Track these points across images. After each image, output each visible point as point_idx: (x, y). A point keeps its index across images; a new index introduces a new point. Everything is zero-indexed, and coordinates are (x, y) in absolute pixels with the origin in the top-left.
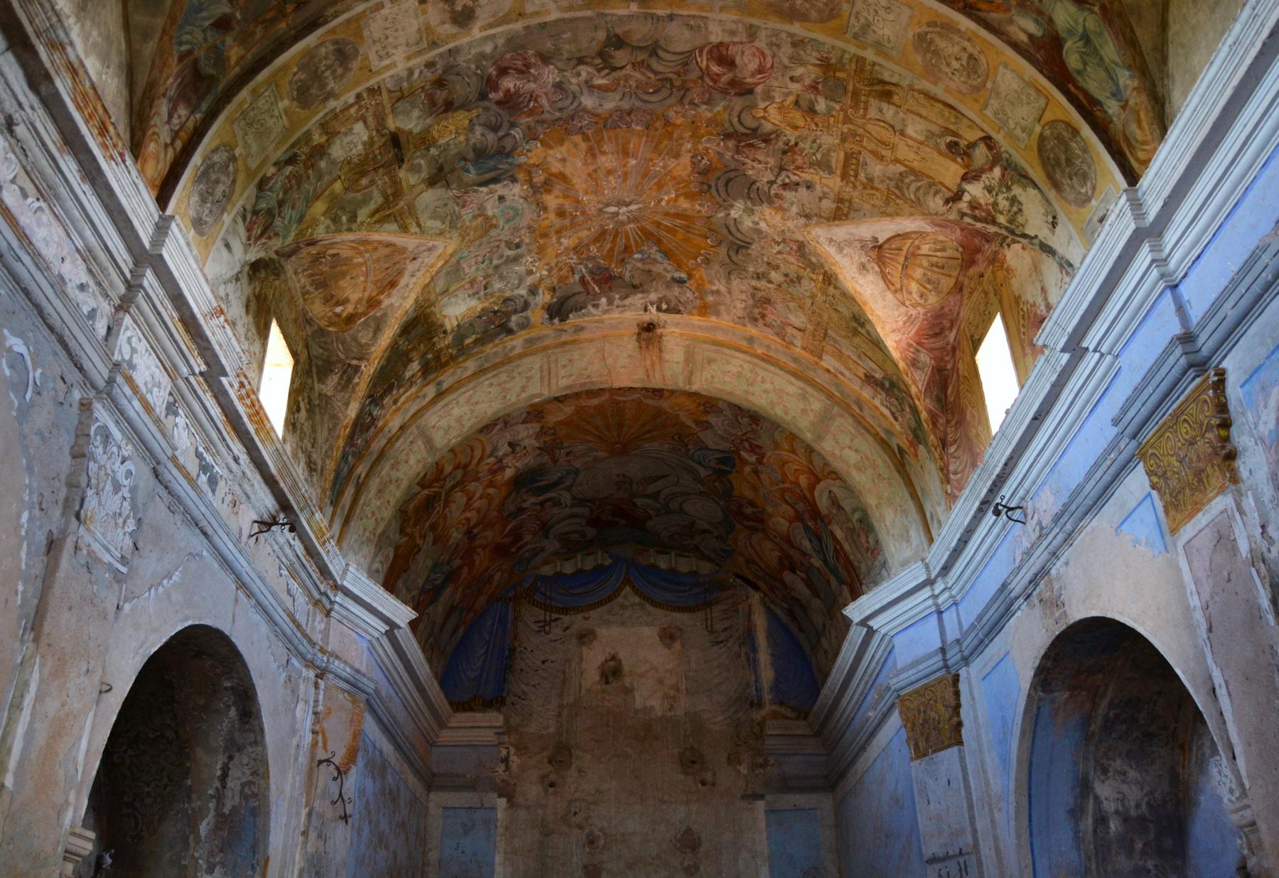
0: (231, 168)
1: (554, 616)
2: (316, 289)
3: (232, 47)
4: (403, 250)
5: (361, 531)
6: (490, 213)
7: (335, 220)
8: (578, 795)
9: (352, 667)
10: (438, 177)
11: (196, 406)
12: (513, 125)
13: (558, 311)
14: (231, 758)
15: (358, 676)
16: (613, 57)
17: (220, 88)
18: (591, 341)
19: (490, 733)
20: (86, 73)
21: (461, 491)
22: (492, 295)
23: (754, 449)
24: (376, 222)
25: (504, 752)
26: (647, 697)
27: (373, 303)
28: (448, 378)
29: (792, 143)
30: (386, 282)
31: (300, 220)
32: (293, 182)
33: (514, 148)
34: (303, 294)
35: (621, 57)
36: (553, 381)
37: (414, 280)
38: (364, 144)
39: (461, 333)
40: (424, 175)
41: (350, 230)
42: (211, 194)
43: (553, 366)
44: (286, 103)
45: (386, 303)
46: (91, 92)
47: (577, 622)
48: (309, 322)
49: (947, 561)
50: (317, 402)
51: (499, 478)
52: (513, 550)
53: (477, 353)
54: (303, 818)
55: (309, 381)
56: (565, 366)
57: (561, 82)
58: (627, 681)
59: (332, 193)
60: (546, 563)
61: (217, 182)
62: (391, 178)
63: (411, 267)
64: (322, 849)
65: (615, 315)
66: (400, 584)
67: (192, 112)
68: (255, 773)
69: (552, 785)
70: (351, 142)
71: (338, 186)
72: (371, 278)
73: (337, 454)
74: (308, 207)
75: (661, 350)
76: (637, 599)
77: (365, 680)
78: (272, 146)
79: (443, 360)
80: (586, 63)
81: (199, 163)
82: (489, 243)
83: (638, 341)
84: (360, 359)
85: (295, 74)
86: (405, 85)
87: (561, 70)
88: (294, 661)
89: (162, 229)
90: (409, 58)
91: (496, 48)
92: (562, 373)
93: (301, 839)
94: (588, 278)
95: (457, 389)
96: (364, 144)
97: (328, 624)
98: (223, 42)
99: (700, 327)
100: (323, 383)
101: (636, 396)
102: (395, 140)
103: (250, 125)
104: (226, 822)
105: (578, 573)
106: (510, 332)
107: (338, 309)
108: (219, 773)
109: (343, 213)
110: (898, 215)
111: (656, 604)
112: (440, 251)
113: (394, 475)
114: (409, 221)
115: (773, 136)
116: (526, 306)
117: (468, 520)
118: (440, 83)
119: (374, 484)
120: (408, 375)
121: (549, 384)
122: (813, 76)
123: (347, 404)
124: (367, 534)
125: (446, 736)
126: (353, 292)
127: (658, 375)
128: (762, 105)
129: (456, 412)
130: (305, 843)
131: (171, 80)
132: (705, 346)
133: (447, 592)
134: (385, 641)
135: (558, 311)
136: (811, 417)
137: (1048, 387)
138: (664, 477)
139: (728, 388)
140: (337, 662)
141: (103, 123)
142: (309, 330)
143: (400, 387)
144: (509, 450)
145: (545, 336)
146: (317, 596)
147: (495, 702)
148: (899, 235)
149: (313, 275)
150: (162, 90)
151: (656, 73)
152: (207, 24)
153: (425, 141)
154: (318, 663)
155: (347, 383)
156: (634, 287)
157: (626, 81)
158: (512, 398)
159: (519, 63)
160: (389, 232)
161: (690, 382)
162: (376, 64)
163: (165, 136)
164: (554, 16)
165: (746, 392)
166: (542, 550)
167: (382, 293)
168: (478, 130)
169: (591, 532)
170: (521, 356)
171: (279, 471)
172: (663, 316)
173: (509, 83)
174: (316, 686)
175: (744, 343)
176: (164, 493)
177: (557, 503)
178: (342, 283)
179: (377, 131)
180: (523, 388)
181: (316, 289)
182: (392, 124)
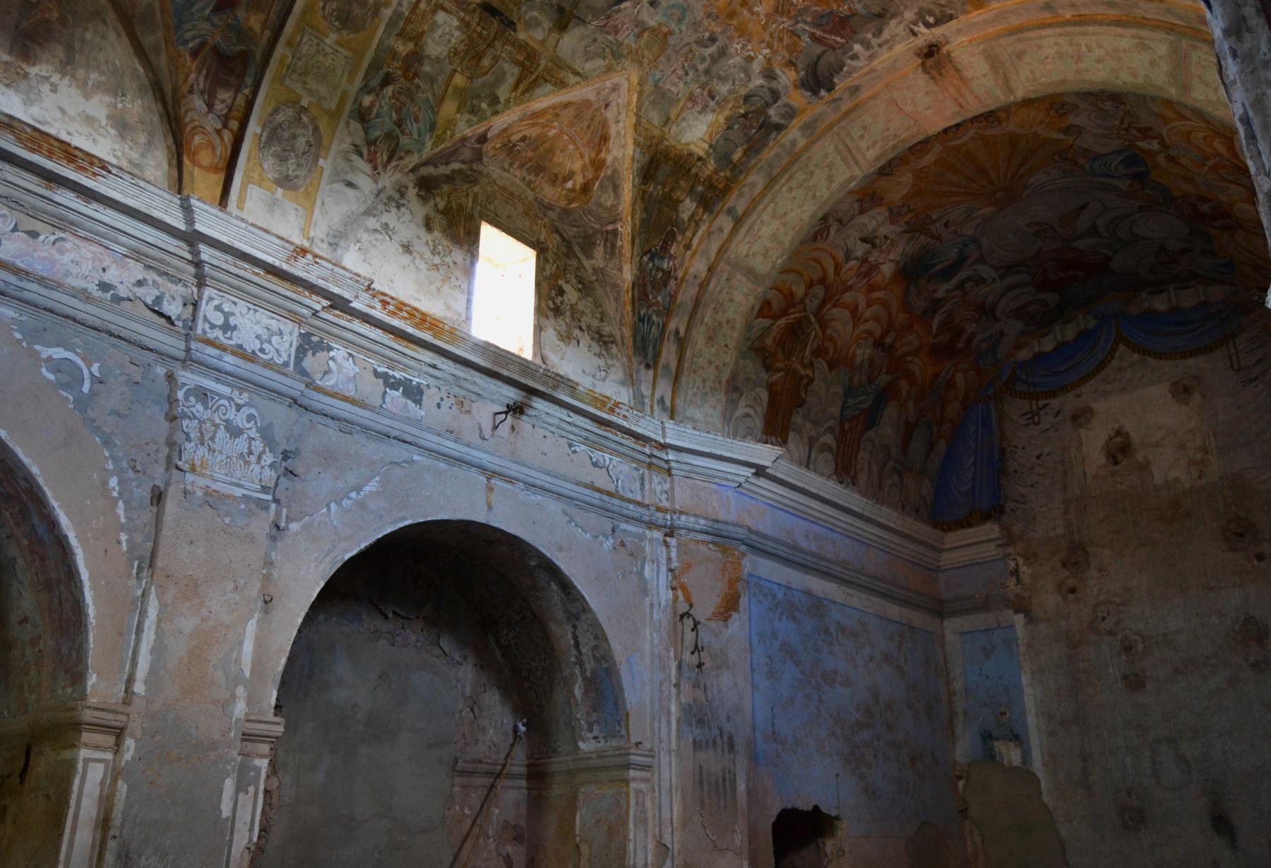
0: (305, 119)
1: (1041, 403)
2: (537, 175)
3: (248, 19)
4: (587, 103)
5: (699, 384)
6: (652, 23)
7: (474, 111)
8: (1101, 598)
9: (706, 519)
13: (817, 80)
14: (575, 627)
15: (720, 526)
17: (258, 58)
18: (873, 97)
19: (992, 546)
20: (20, 121)
21: (835, 306)
22: (725, 99)
23: (1147, 133)
24: (523, 93)
25: (1012, 564)
26: (1168, 468)
27: (598, 165)
28: (738, 201)
30: (597, 141)
31: (433, 127)
32: (402, 98)
36: (859, 158)
37: (621, 125)
38: (458, 28)
39: (721, 153)
40: (547, 24)
41: (496, 113)
42: (293, 150)
43: (848, 141)
44: (332, 38)
45: (609, 159)
46: (36, 134)
47: (1068, 402)
48: (550, 207)
50: (594, 278)
51: (877, 278)
52: (960, 345)
53: (756, 164)
54: (674, 671)
55: (574, 262)
56: (862, 137)
58: (1140, 456)
59: (456, 88)
60: (1019, 347)
61: (294, 137)
62: (513, 44)
63: (610, 114)
64: (702, 698)
65: (885, 56)
66: (797, 419)
67: (237, 91)
68: (596, 637)
69: (1073, 591)
70: (444, 34)
71: (459, 80)
72: (579, 143)
73: (629, 319)
74: (435, 113)
75: (957, 70)
76: (1136, 357)
77: (730, 528)
78: (344, 80)
79: (721, 186)
81: (258, 131)
82: (677, 52)
83: (926, 72)
84: (614, 222)
85: (324, 8)
88: (624, 526)
89: (187, 209)
92: (864, 144)
93: (674, 690)
94: (818, 33)
95: (755, 207)
96: (458, 28)
97: (672, 482)
98: (236, 19)
99: (986, 22)
100: (592, 258)
101: (972, 132)
103: (305, 73)
104: (591, 684)
105: (1060, 347)
106: (779, 128)
107: (569, 184)
108: (572, 642)
109: (479, 101)
111: (1159, 356)
112: (626, 85)
113: (721, 317)
114: (562, 74)
116: (775, 95)
117: (869, 333)
119: (699, 336)
120: (685, 216)
121: (856, 162)
123: (620, 270)
124: (709, 384)
125: (947, 559)
126: (573, 161)
127: (971, 100)
129: (766, 231)
130: (679, 693)
131: (193, 76)
132: (1003, 41)
133: (890, 411)
134: (763, 482)
135: (817, 80)
136: (1165, 66)
138: (1084, 207)
139: (1056, 77)
140: (683, 518)
141: (66, 152)
142: (553, 215)
143: (683, 232)
144: (868, 246)
145: (821, 115)
146: (648, 460)
147: (993, 512)
149: (521, 167)
150: (185, 89)
152: (207, 12)
154: (660, 522)
155: (612, 251)
156: (879, 16)
158: (823, 193)
160: (545, 95)
161: (1010, 90)
163: (212, 123)
165: (1078, 72)
166: (1002, 334)
167: (601, 151)
169: (1052, 298)
170: (806, 148)
172: (938, 31)
174: (666, 544)
175: (1047, 15)
176: (329, 421)
177: (980, 281)
178: (558, 158)
179: (464, 10)
180: (830, 179)
181: (537, 175)
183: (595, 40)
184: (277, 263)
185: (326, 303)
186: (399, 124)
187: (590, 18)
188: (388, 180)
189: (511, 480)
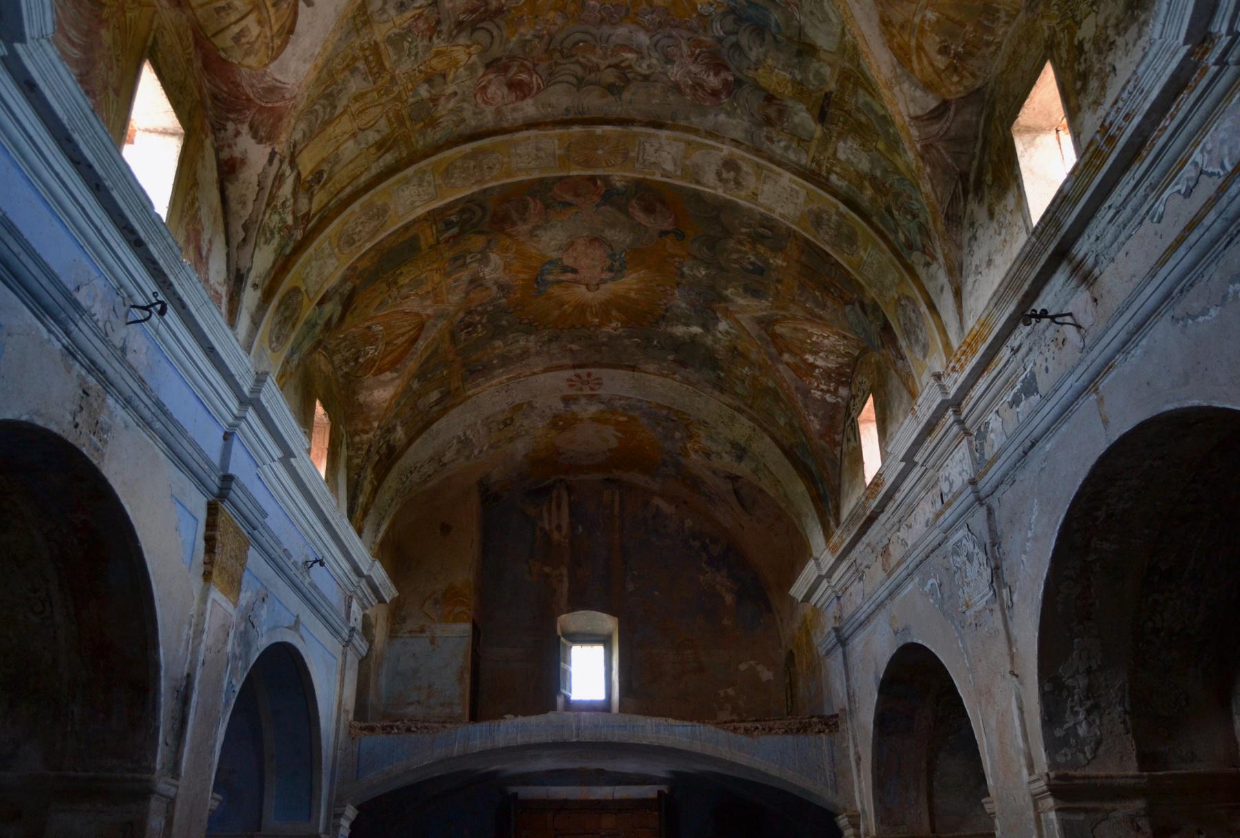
2: (998, 11)
10: (806, 50)
11: (982, 404)
12: (720, 40)
16: (619, 78)
29: (434, 38)
33: (725, 15)
34: (1014, 17)
35: (610, 77)
40: (816, 65)
49: (217, 354)
57: (666, 63)
80: (641, 75)
86: (794, 145)
87: (665, 74)
90: (779, 174)
91: (716, 115)
102: (822, 117)
110: (318, 79)
115: (454, 33)
118: (768, 121)
122: (440, 108)
128: (474, 58)
137: (233, 371)
148: (291, 31)
149: (989, 30)
151: (578, 62)
153: (801, 90)
157: (605, 54)
159: (700, 93)
162: (803, 193)
164: (664, 133)
168: (753, 55)
171: (1015, 293)
173: (713, 81)
176: (1001, 489)
181: (998, 11)
182: (818, 131)
183: (812, 13)
184: (918, 431)
185: (950, 412)
186: (915, 216)
187: (795, 23)
188: (981, 213)
189: (1107, 366)
